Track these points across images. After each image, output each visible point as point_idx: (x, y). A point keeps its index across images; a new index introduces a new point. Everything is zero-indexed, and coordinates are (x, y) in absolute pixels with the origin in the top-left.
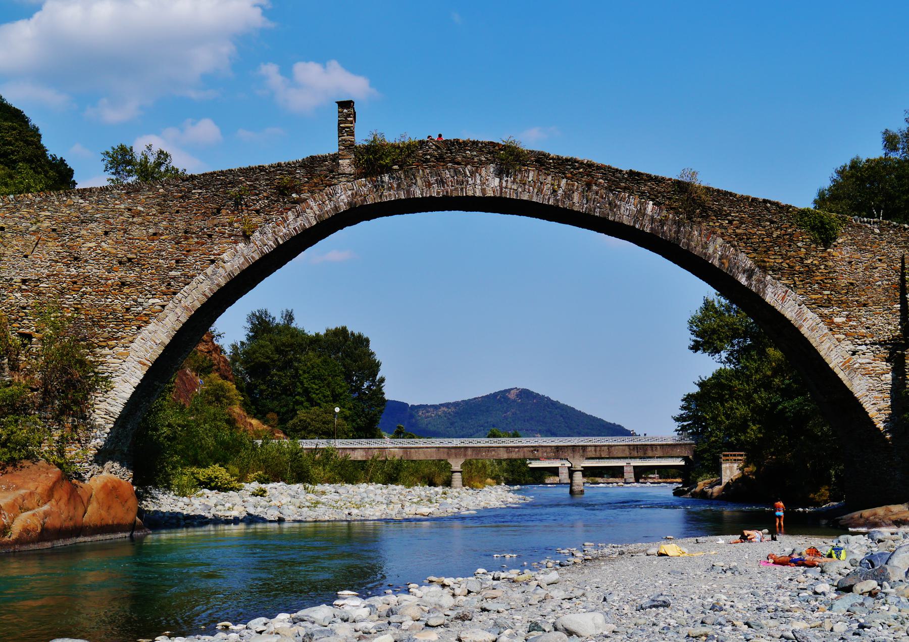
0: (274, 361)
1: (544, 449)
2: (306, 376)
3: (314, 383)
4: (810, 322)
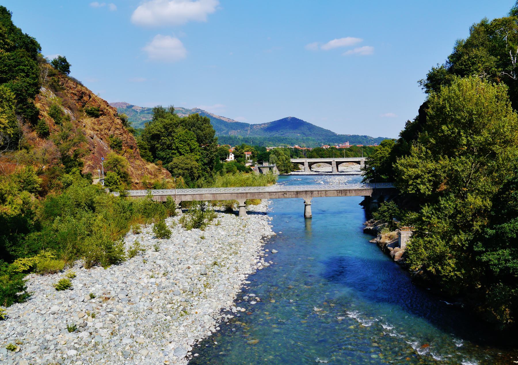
0: (162, 133)
1: (290, 193)
2: (177, 140)
3: (181, 144)
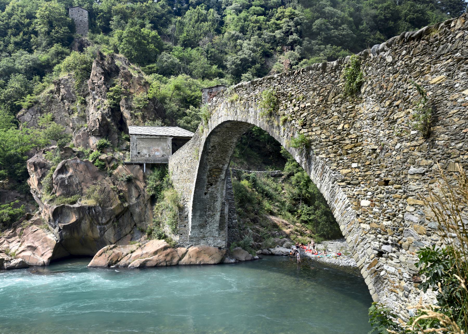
4: (341, 203)
